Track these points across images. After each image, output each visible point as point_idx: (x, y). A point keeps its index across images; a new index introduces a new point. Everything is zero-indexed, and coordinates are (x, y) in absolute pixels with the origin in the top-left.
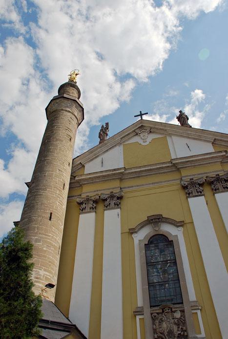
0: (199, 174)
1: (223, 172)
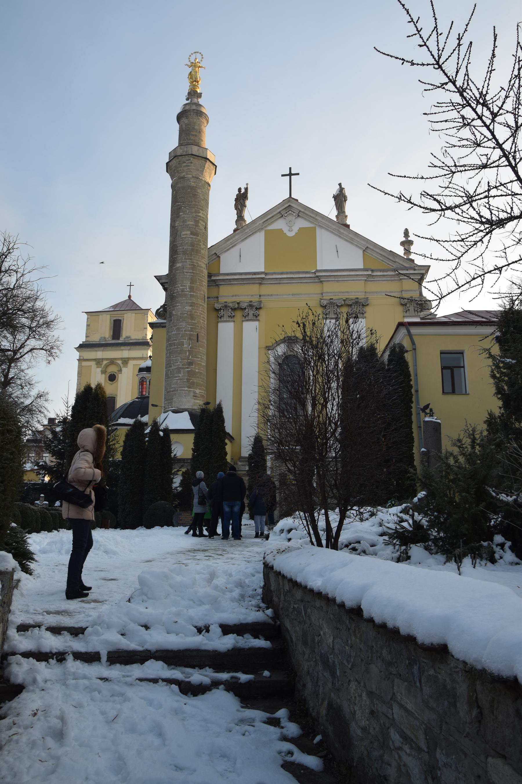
0: (340, 292)
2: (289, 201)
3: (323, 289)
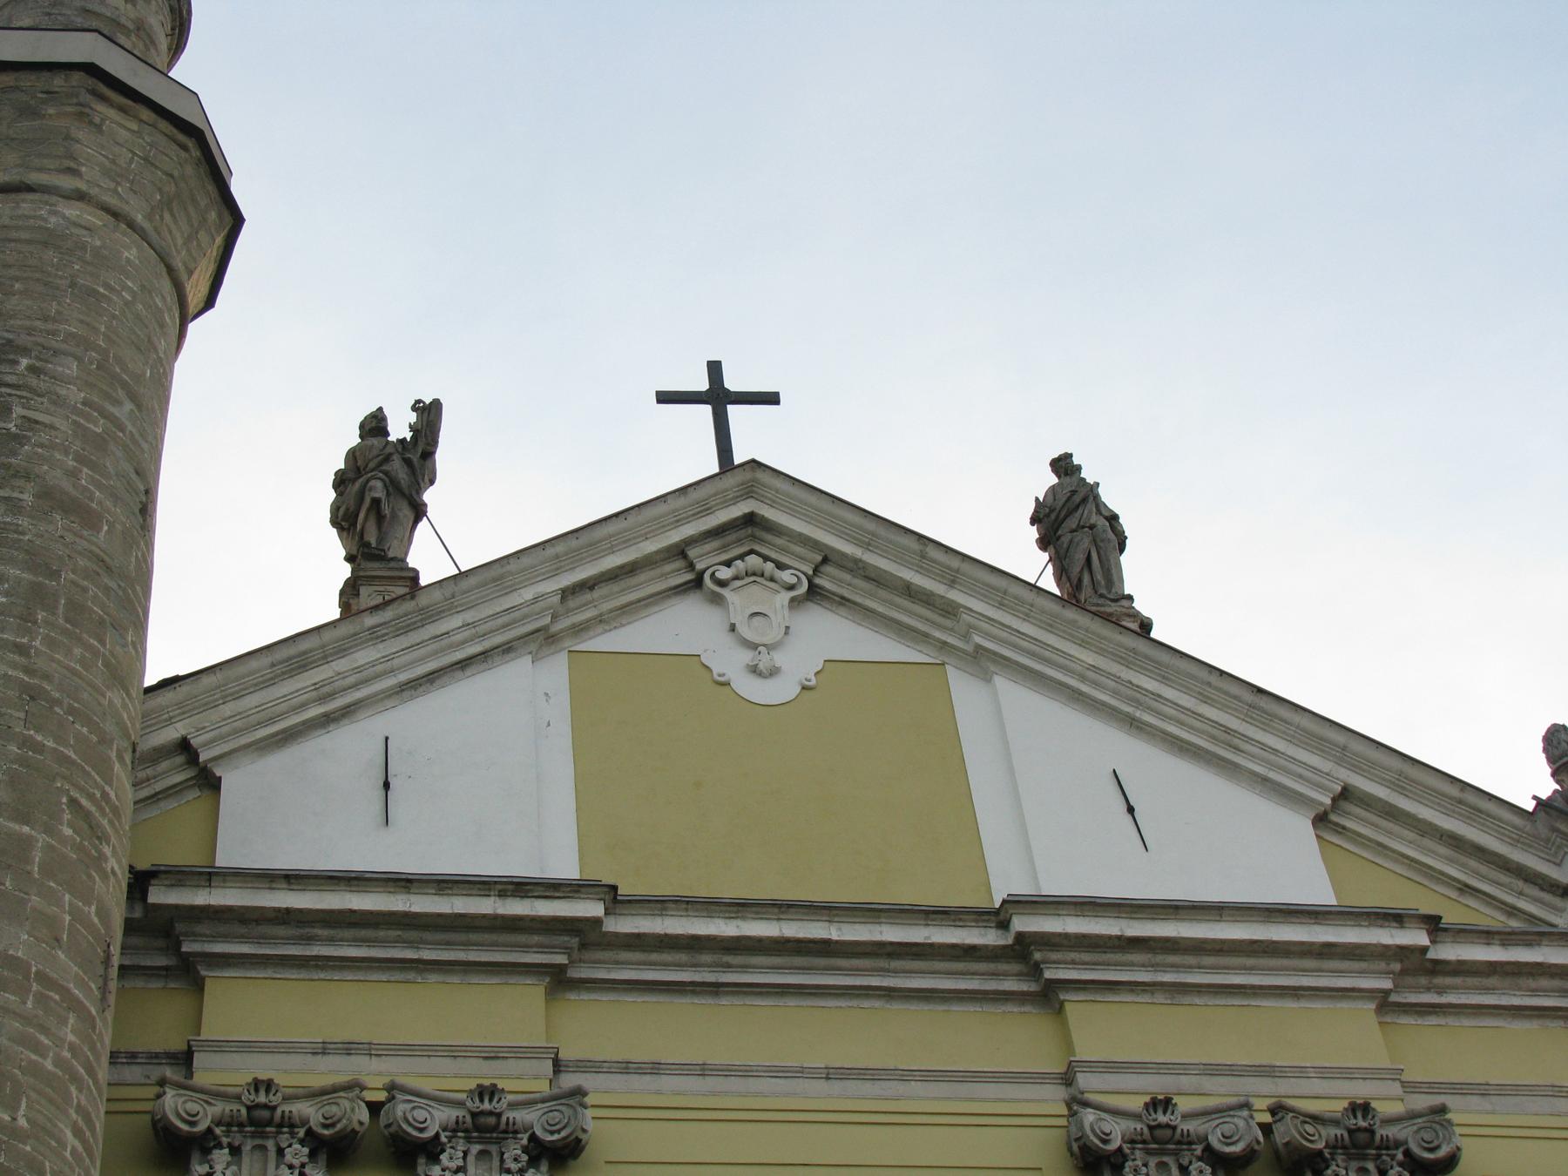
1: (1396, 1089)
3: (1068, 1045)
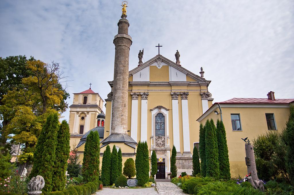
2: (159, 56)
